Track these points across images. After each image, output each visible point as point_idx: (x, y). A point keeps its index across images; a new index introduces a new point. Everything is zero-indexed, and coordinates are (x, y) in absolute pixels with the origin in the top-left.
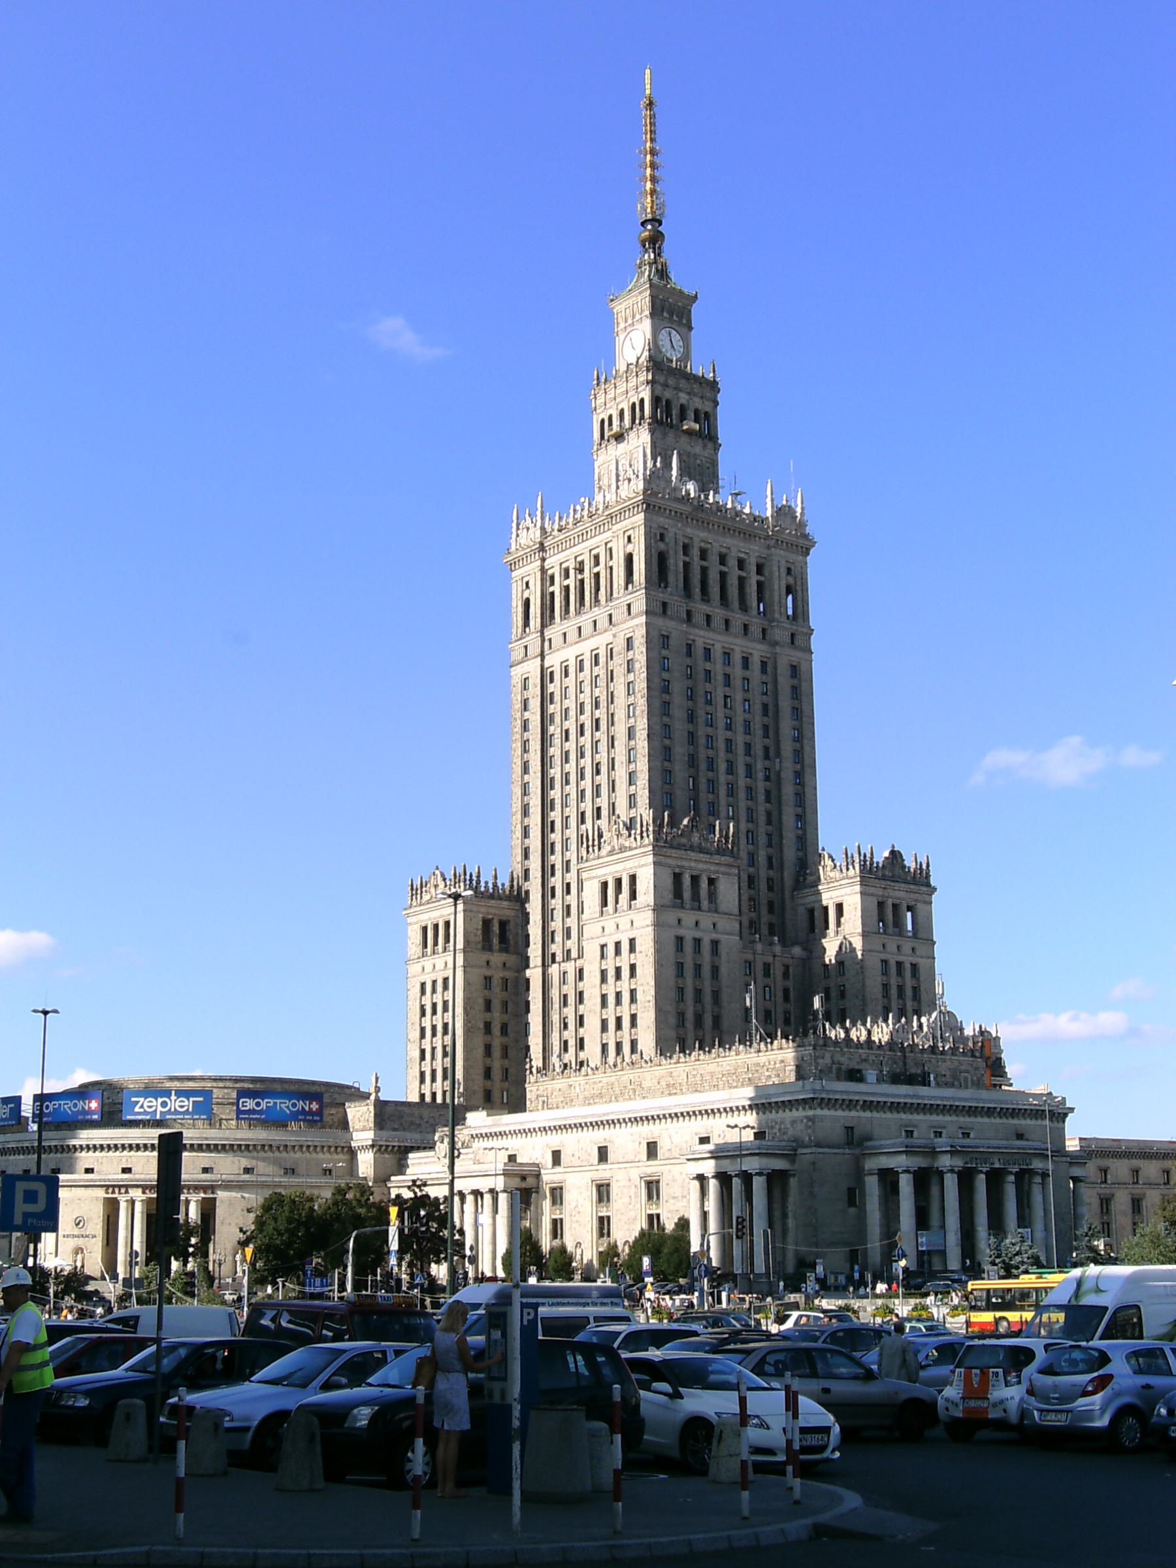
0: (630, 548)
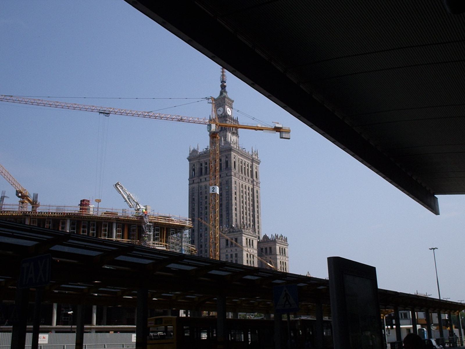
0: (227, 159)
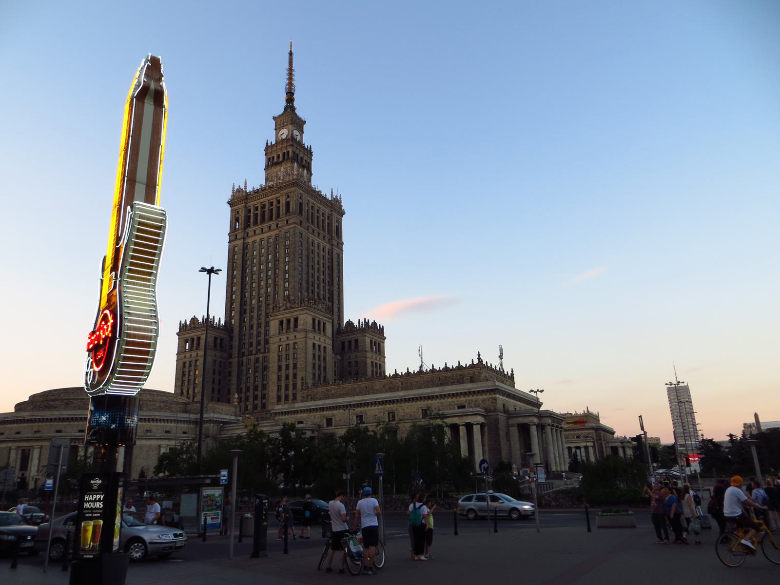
0: (288, 199)
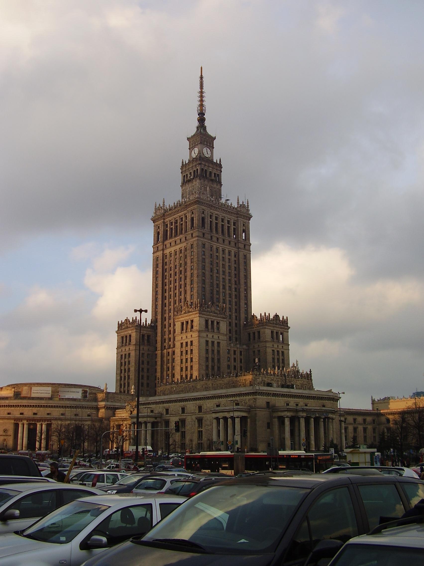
0: (193, 215)
